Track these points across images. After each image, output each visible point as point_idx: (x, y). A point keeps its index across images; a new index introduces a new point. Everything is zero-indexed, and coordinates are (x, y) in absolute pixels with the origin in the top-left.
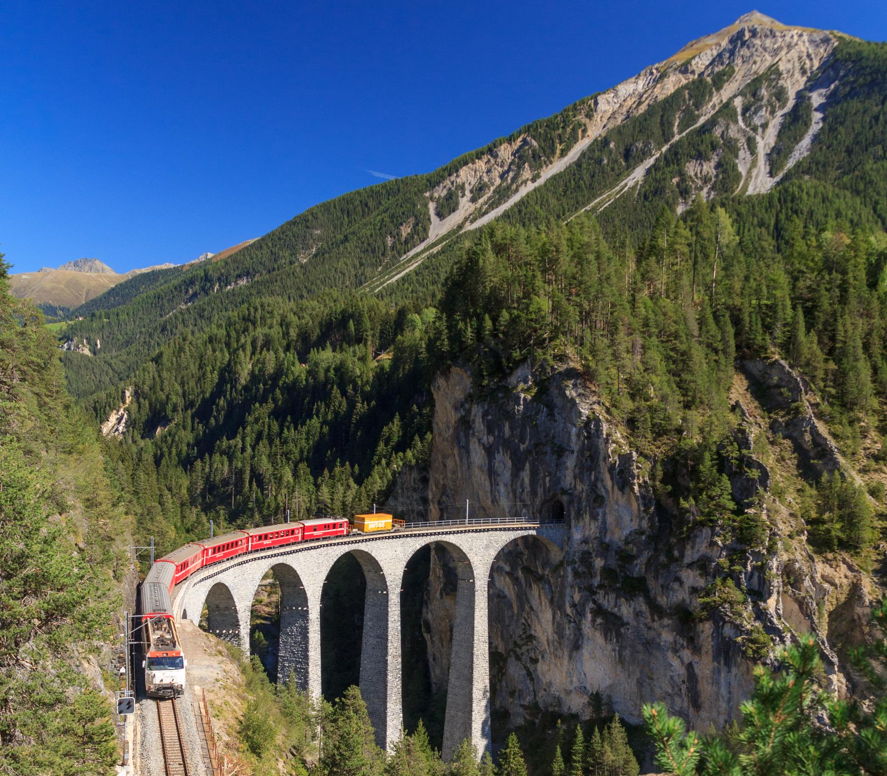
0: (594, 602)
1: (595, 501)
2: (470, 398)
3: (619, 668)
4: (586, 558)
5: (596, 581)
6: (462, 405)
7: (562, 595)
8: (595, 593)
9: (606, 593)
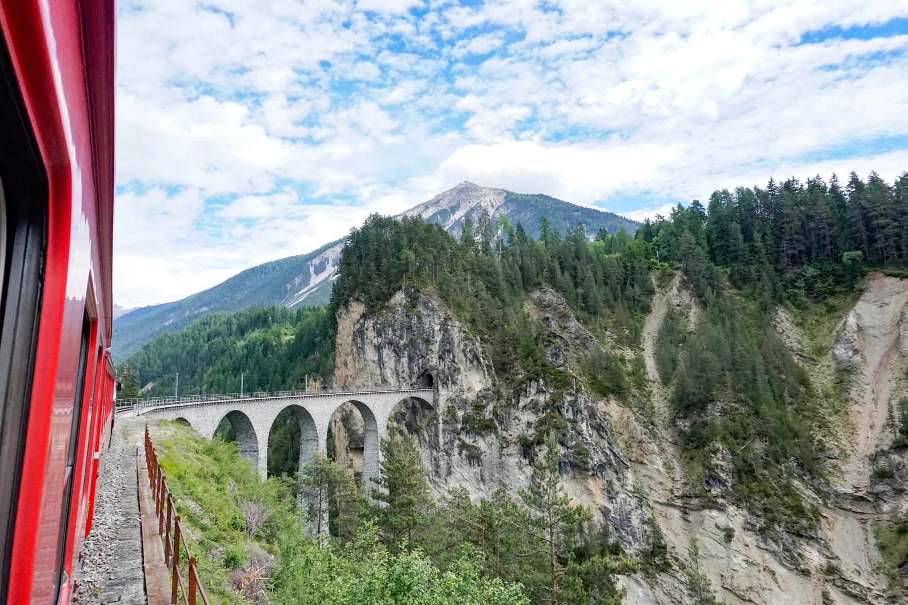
0: (460, 439)
1: (455, 371)
2: (364, 316)
3: (482, 486)
4: (451, 411)
5: (459, 426)
6: (358, 321)
7: (437, 435)
8: (459, 434)
9: (467, 433)
